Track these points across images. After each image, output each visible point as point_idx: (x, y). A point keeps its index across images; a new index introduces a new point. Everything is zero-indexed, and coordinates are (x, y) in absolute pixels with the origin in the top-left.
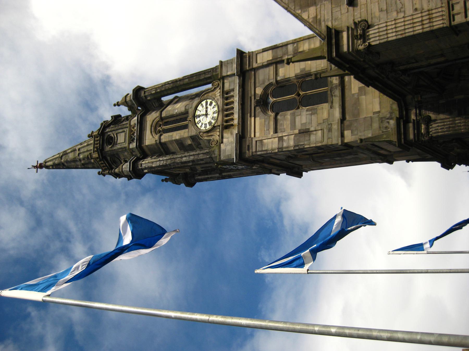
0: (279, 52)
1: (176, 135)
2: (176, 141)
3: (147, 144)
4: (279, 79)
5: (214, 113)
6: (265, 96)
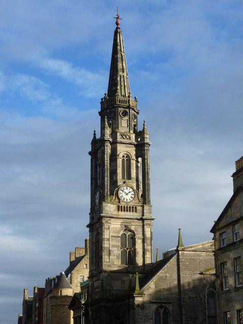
0: (148, 241)
1: (120, 170)
2: (116, 170)
3: (118, 148)
4: (136, 239)
5: (127, 199)
6: (130, 231)
